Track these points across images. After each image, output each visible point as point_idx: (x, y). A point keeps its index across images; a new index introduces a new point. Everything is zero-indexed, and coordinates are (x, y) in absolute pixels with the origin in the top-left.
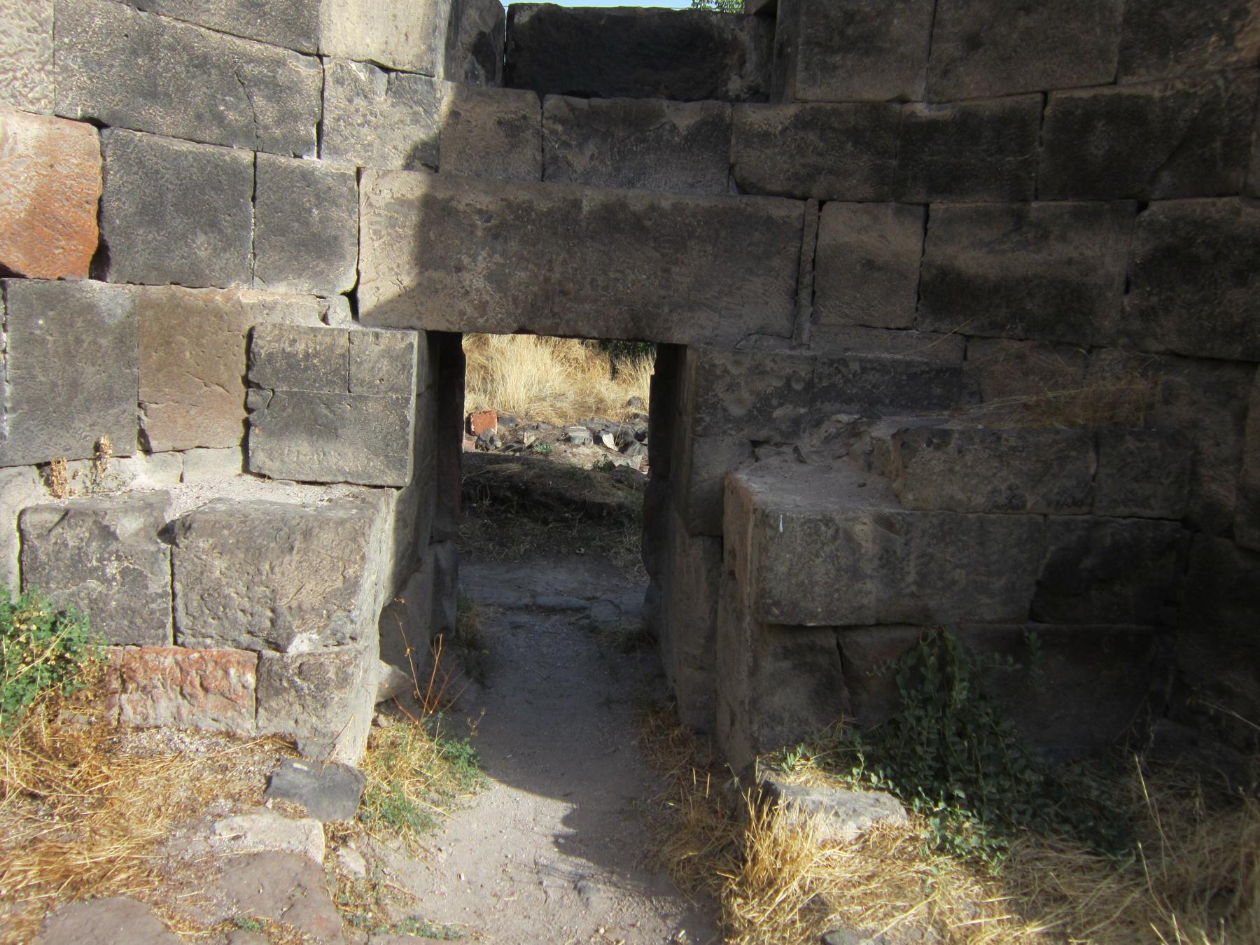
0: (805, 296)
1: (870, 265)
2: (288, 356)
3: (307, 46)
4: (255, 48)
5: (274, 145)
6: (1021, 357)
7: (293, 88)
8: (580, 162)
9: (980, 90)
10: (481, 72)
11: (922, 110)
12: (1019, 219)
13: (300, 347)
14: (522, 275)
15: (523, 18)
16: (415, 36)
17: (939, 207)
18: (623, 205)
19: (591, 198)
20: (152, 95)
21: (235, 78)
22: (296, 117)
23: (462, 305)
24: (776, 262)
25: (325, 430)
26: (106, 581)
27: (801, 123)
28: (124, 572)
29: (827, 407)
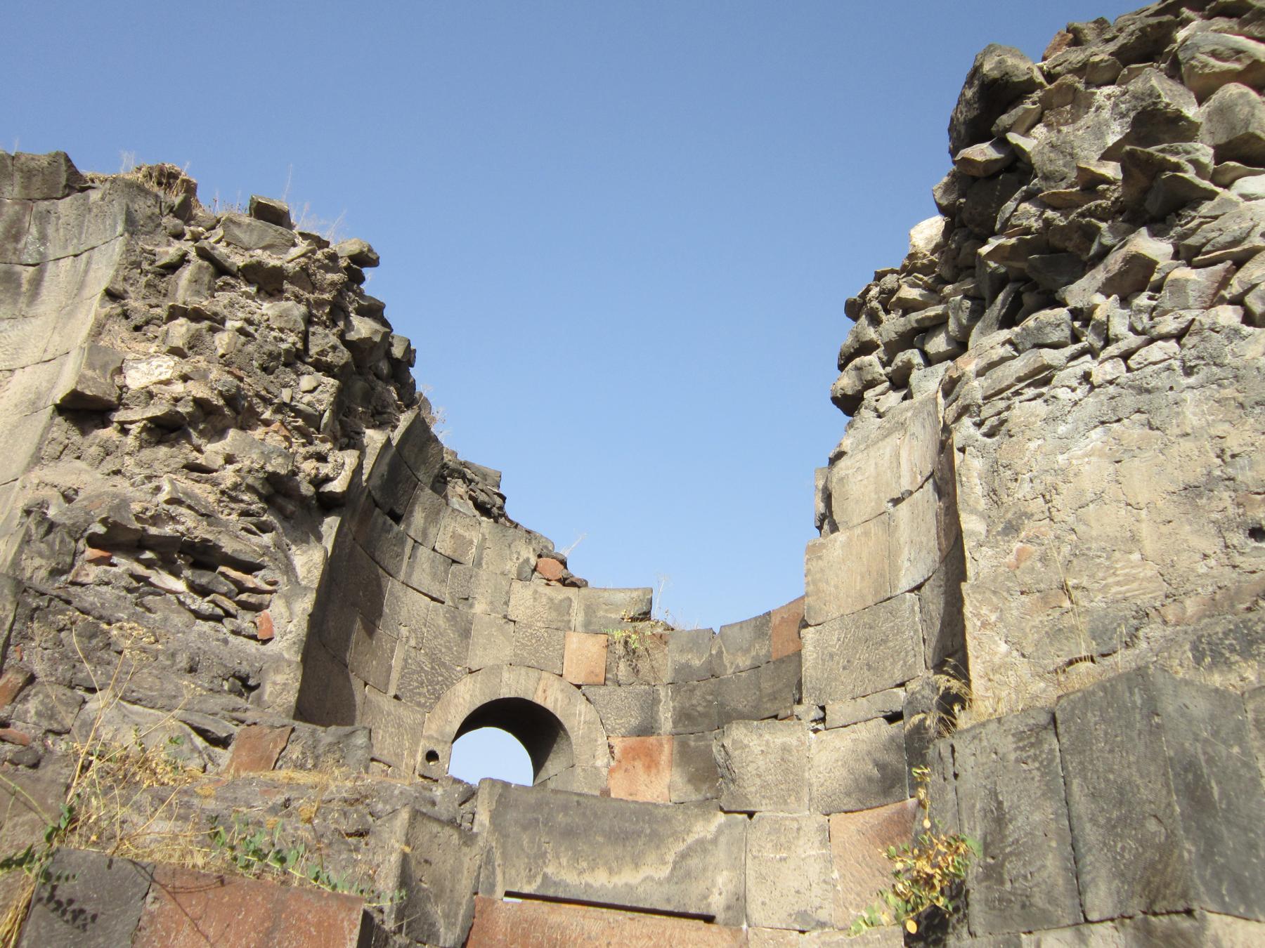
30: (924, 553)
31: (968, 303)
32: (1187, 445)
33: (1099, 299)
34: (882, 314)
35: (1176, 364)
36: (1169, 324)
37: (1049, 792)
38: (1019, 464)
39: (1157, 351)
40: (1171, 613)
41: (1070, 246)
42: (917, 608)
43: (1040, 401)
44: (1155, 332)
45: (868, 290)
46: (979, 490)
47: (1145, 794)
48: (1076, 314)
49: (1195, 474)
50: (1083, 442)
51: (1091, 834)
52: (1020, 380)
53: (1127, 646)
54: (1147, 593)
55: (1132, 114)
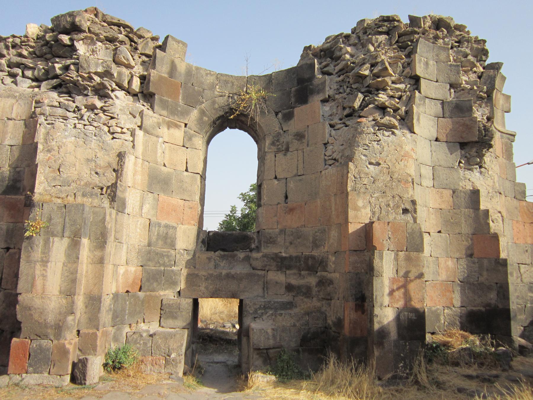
0: (265, 289)
1: (277, 283)
2: (169, 304)
3: (173, 248)
4: (165, 250)
5: (167, 266)
6: (302, 299)
7: (171, 256)
8: (222, 264)
9: (293, 252)
10: (203, 246)
11: (284, 255)
12: (300, 274)
13: (171, 302)
14: (211, 287)
15: (211, 234)
16: (192, 244)
17: (288, 272)
18: (230, 273)
19: (224, 272)
20: (149, 260)
21: (162, 255)
22: (171, 261)
23: (200, 293)
24: (260, 282)
25: (175, 318)
26: (140, 344)
27: (263, 256)
28: (144, 343)
29: (268, 310)
30: (16, 138)
31: (43, 71)
32: (90, 150)
33: (83, 107)
34: (10, 48)
35: (94, 133)
36: (95, 124)
37: (62, 217)
38: (54, 137)
39: (91, 128)
40: (78, 182)
41: (80, 87)
42: (9, 150)
43: (63, 124)
44: (92, 124)
45: (8, 38)
46: (42, 137)
47: (78, 221)
48: (77, 107)
49: (90, 158)
50: (70, 139)
51: (67, 225)
52: (60, 116)
53: (68, 186)
54: (75, 177)
55: (105, 69)
